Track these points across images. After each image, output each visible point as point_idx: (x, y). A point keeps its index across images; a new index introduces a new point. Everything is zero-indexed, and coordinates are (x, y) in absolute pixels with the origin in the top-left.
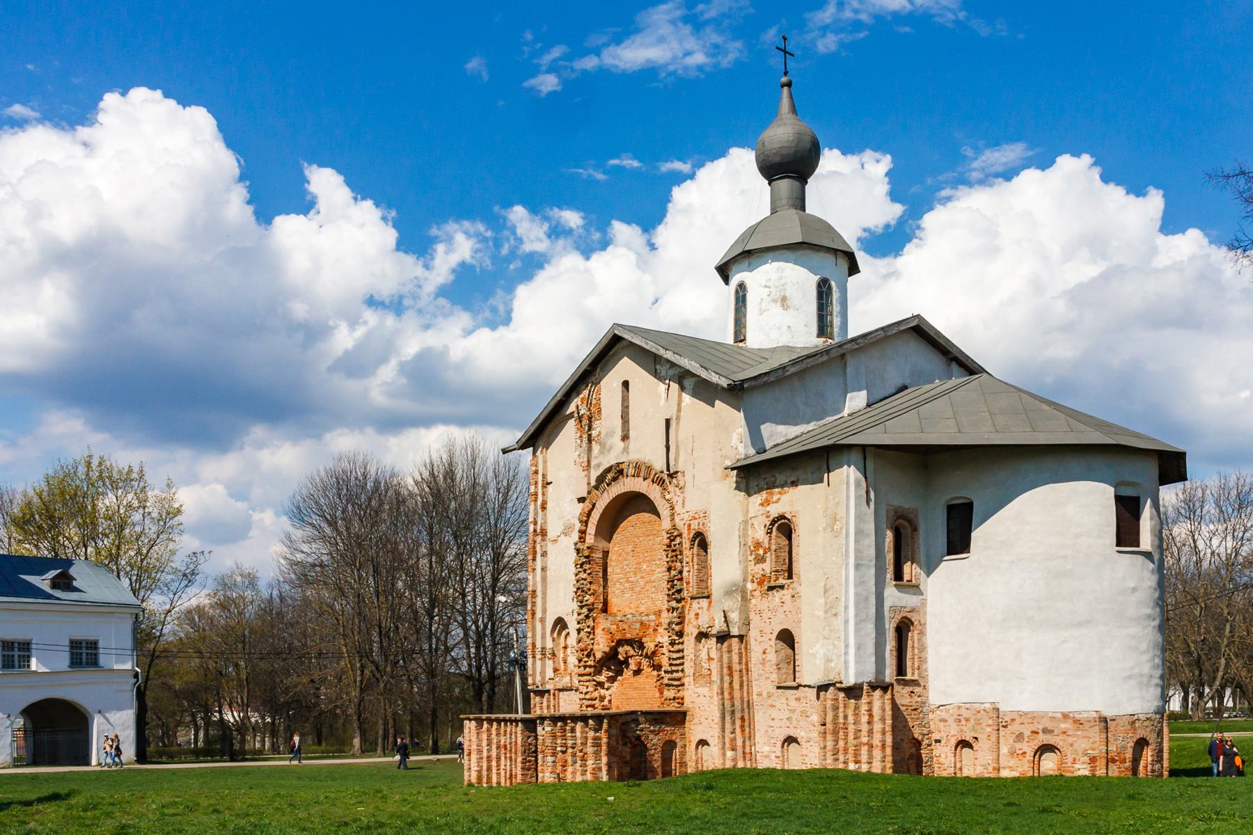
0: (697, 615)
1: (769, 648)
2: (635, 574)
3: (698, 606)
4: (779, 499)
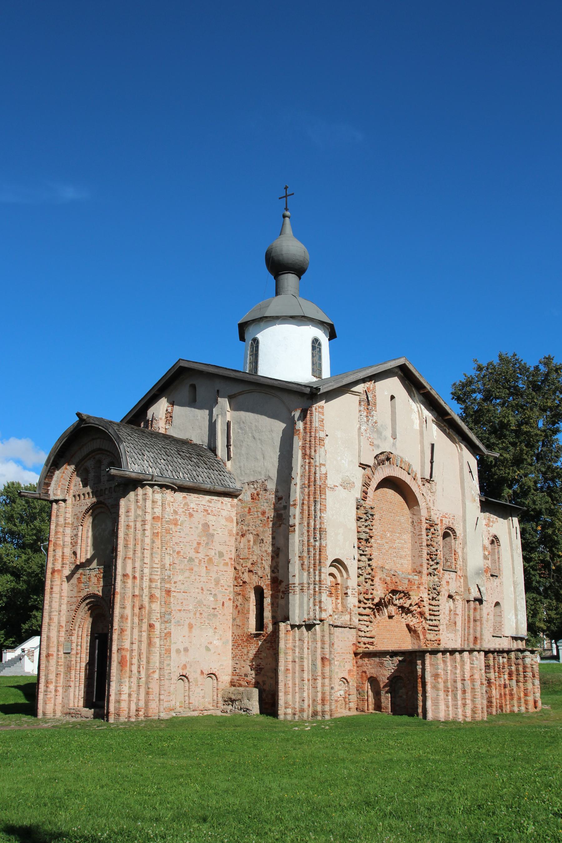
0: (448, 582)
1: (491, 612)
2: (382, 538)
3: (448, 577)
4: (492, 526)
